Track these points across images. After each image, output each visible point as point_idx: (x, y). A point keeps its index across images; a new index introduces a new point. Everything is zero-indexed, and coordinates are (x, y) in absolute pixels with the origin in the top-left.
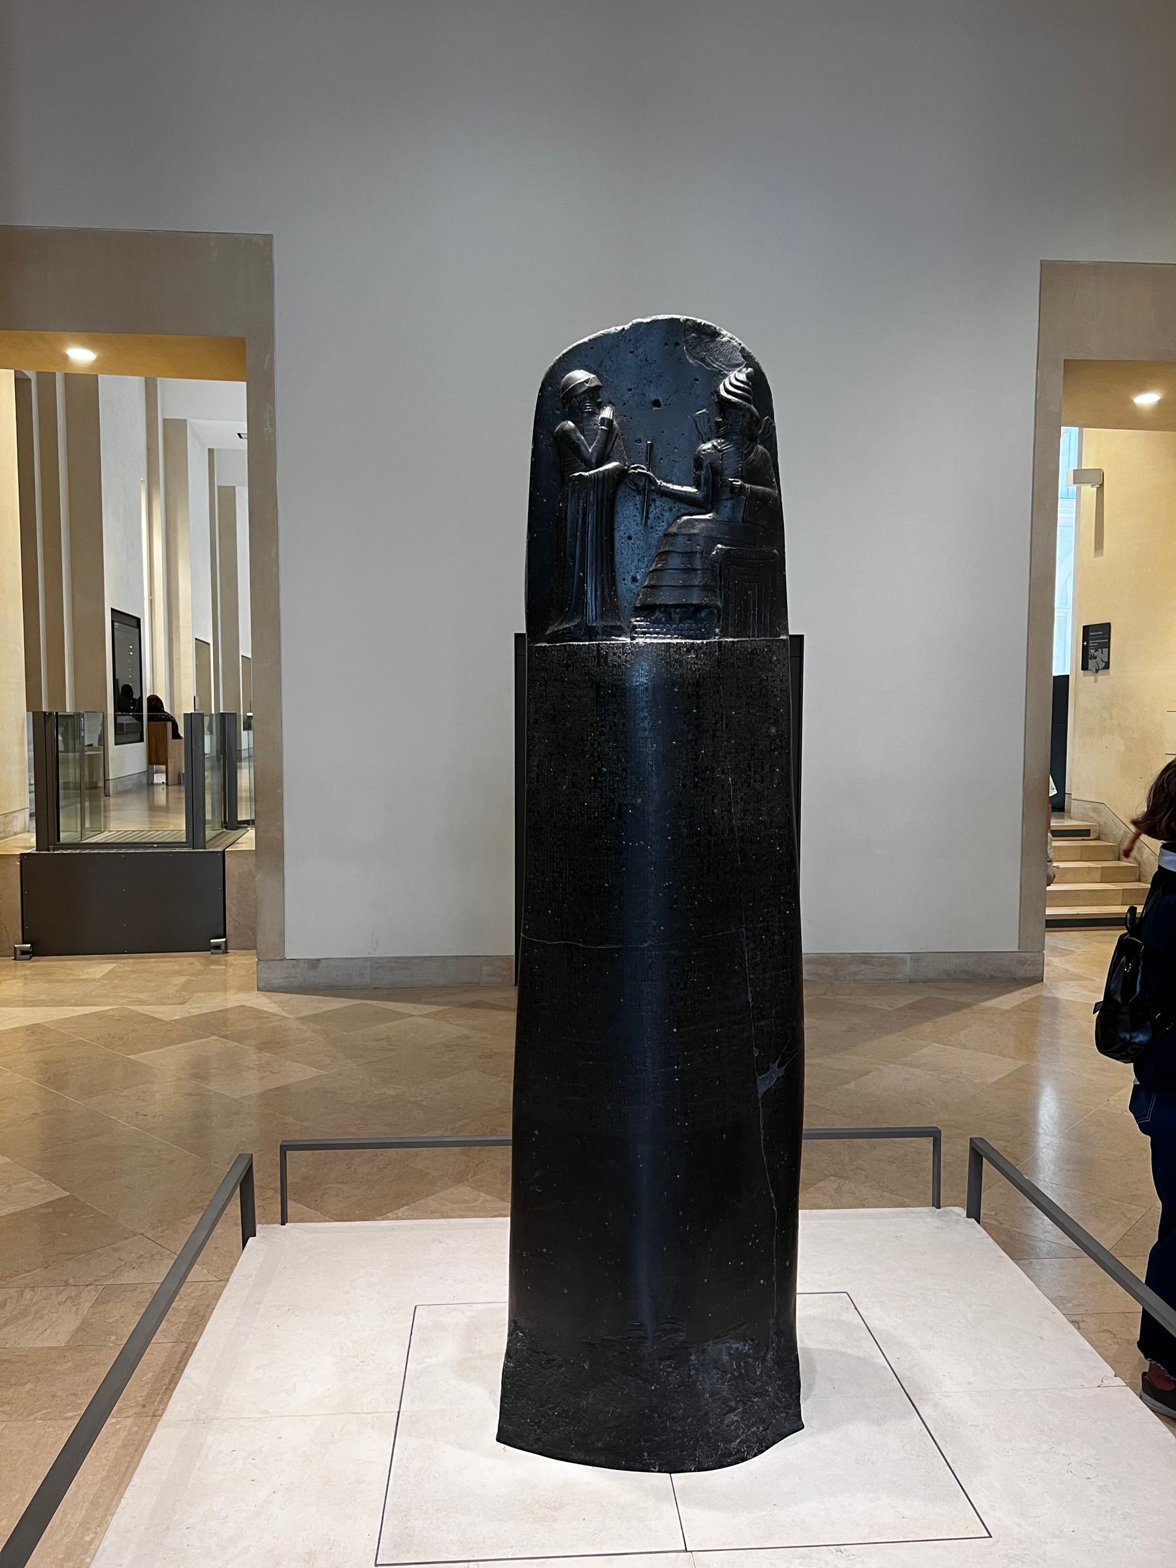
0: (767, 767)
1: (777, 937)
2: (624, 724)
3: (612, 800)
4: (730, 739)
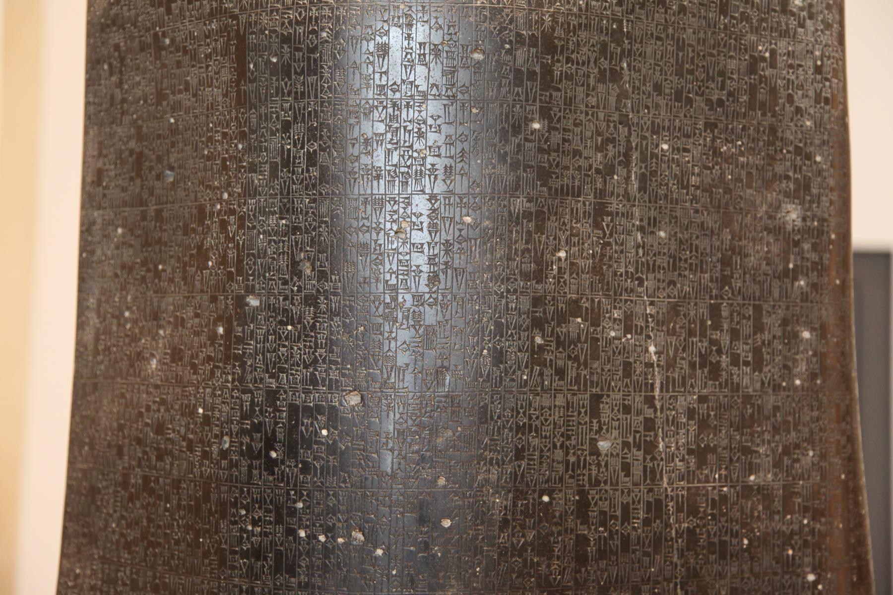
0: (772, 322)
2: (311, 159)
3: (272, 396)
4: (654, 223)
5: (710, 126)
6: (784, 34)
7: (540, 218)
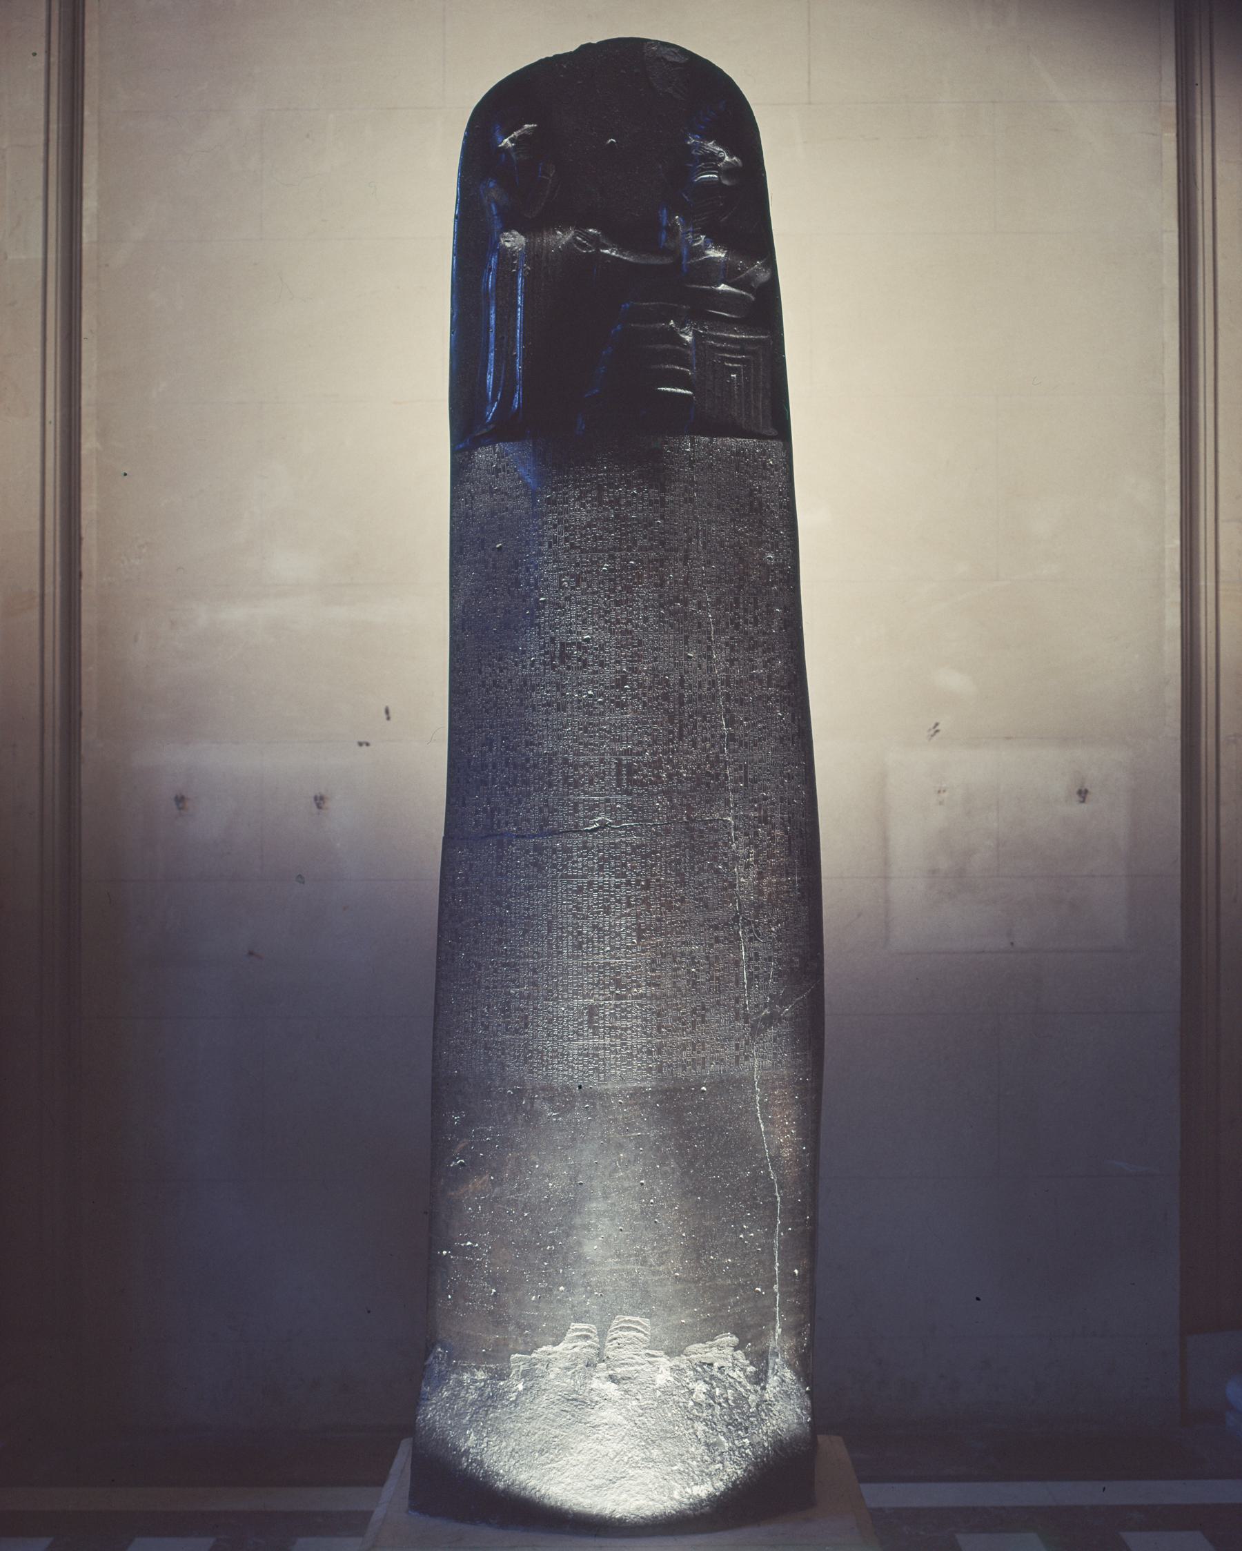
1: (778, 832)
3: (553, 640)
4: (710, 563)
5: (732, 520)
6: (765, 478)
7: (661, 562)
